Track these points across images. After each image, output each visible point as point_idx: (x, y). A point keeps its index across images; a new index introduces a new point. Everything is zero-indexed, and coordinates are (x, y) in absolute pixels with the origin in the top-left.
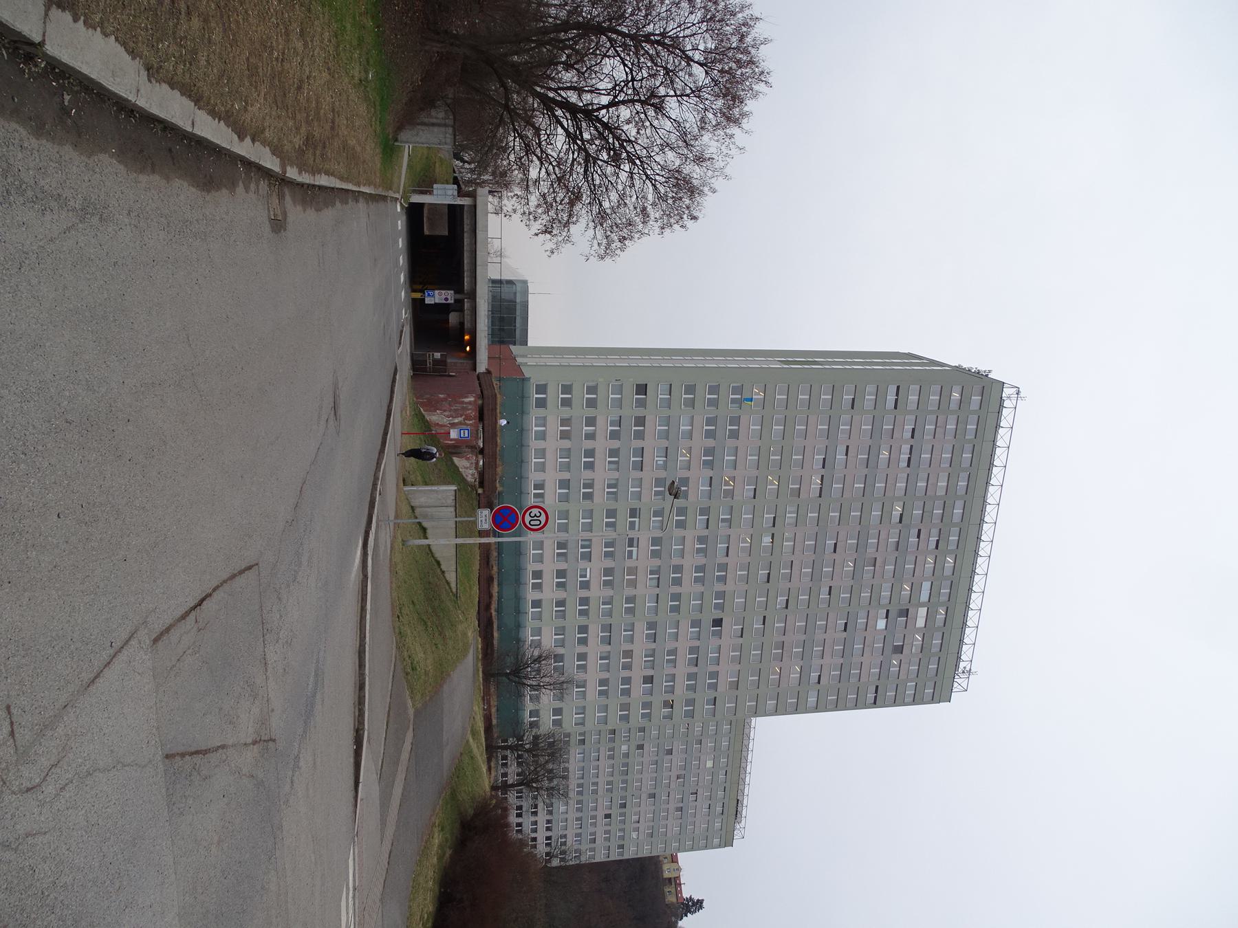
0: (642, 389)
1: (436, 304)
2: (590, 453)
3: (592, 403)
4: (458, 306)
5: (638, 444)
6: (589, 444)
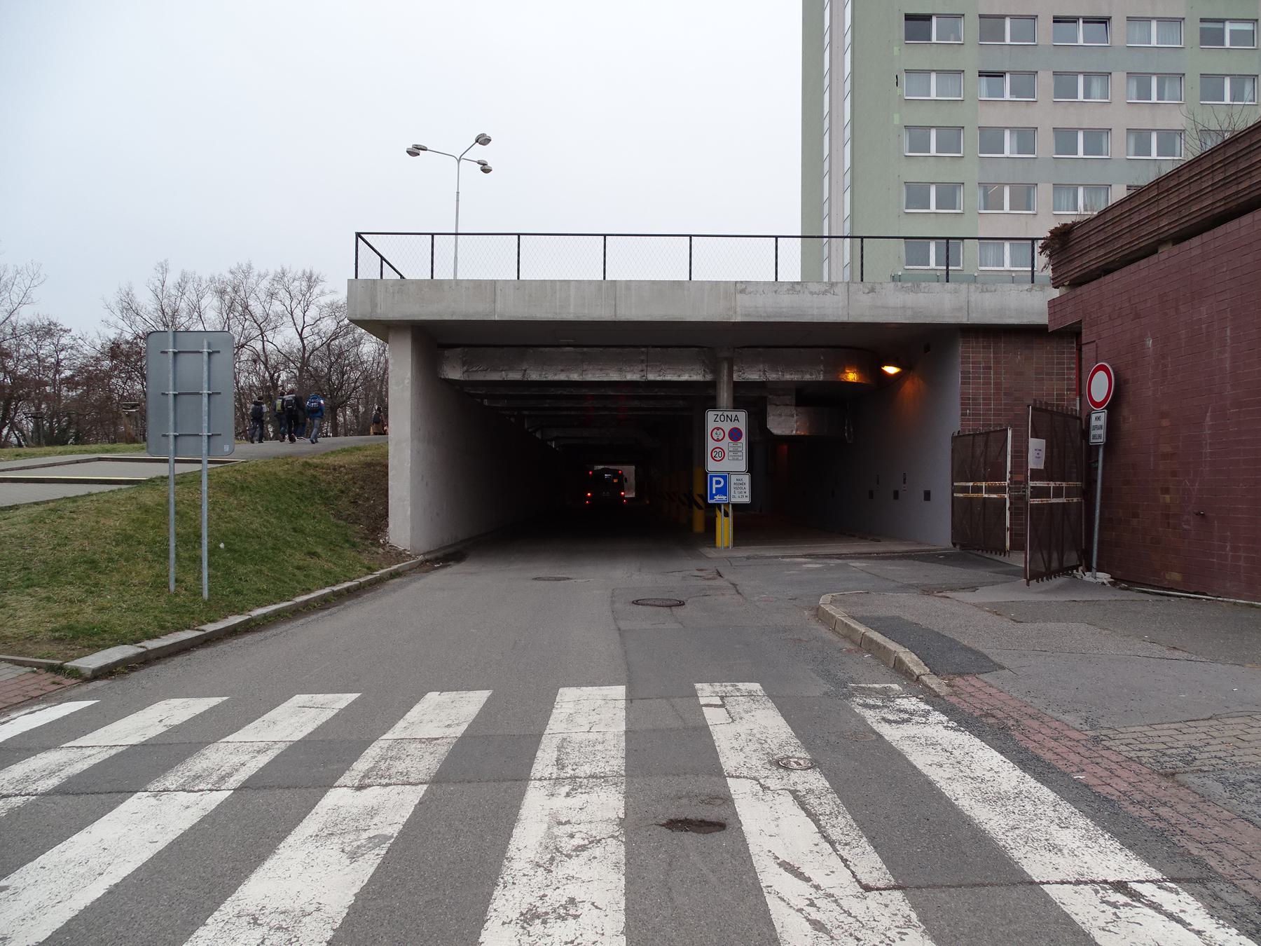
0: (917, 23)
1: (751, 469)
2: (1065, 137)
3: (951, 137)
6: (1045, 145)
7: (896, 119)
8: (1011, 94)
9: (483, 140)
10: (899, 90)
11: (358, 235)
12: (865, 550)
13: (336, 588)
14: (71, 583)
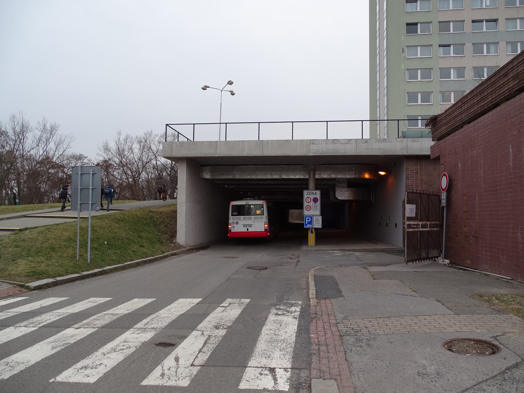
0: (412, 27)
1: (322, 214)
3: (427, 73)
4: (326, 188)
5: (468, 27)
7: (403, 66)
8: (454, 53)
9: (230, 83)
10: (404, 54)
11: (167, 125)
12: (363, 248)
13: (144, 260)
14: (42, 256)
